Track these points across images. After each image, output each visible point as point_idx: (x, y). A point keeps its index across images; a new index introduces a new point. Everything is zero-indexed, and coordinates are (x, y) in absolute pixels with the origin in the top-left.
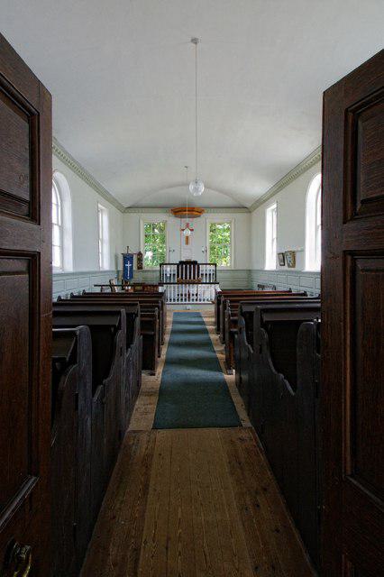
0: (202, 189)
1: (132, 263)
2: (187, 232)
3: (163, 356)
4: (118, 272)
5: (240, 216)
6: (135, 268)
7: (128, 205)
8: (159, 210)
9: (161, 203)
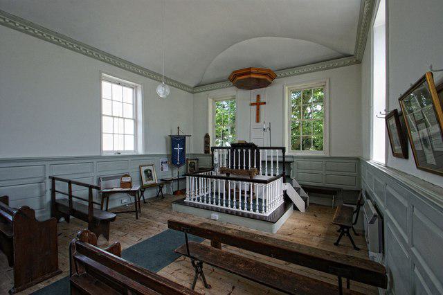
7: (193, 86)
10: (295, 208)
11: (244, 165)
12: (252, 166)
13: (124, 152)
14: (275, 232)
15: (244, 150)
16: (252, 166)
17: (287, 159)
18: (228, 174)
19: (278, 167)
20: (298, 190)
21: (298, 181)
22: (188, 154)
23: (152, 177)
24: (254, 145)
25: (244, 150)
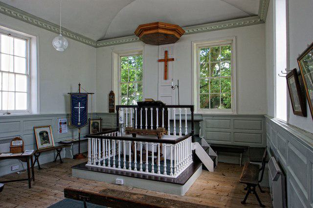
7: (96, 39)
10: (204, 168)
12: (160, 125)
13: (15, 111)
14: (183, 194)
15: (152, 109)
16: (160, 125)
17: (195, 118)
18: (134, 135)
19: (186, 126)
20: (206, 149)
21: (206, 140)
22: (90, 114)
23: (48, 140)
24: (162, 103)
25: (152, 109)
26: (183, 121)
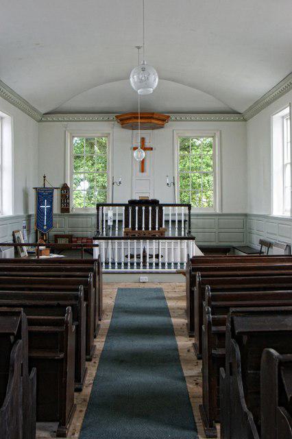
0: (155, 81)
1: (51, 203)
2: (140, 155)
3: (87, 391)
4: (29, 216)
5: (229, 127)
6: (56, 210)
7: (43, 111)
8: (96, 117)
9: (103, 105)
11: (150, 226)
15: (144, 208)
25: (144, 208)
26: (180, 222)
